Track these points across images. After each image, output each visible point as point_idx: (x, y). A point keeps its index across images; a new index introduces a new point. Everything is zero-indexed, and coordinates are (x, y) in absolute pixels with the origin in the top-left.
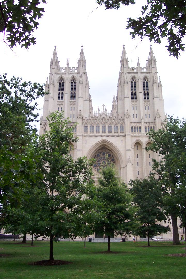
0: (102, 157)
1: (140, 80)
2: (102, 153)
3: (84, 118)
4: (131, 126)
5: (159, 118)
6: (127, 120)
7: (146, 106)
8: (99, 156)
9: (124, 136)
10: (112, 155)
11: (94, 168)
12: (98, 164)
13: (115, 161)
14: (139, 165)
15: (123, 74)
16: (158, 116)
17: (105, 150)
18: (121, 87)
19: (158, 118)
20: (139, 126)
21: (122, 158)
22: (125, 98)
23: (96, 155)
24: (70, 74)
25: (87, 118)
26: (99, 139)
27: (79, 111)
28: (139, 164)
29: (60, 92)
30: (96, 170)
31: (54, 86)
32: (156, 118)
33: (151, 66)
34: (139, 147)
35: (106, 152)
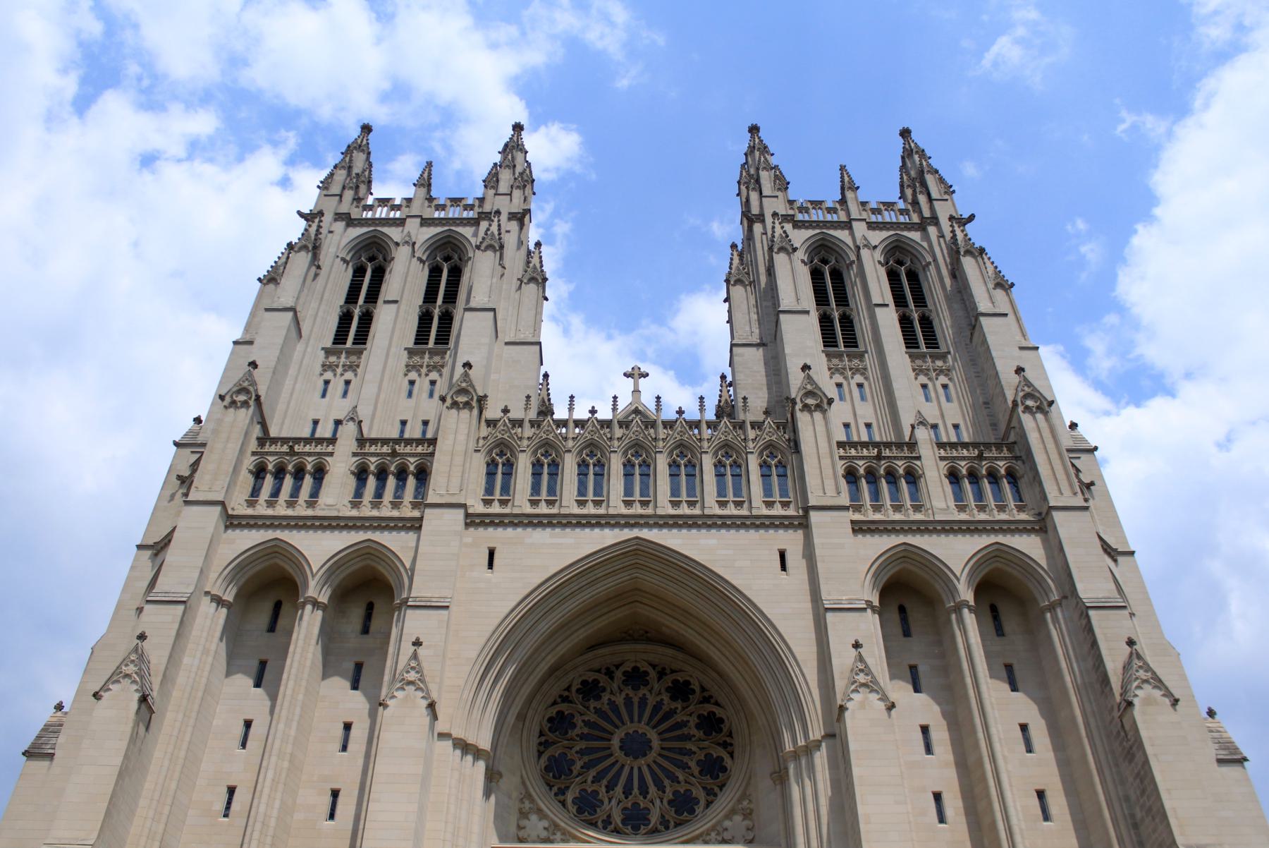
0: (620, 700)
1: (865, 253)
2: (619, 674)
3: (492, 412)
4: (841, 467)
5: (1039, 416)
7: (923, 379)
8: (598, 698)
10: (703, 689)
11: (551, 787)
12: (581, 753)
13: (730, 735)
16: (1030, 403)
17: (639, 647)
20: (901, 467)
23: (568, 689)
24: (426, 222)
25: (512, 415)
26: (609, 537)
27: (459, 370)
30: (570, 797)
33: (922, 199)
34: (916, 616)
35: (654, 666)
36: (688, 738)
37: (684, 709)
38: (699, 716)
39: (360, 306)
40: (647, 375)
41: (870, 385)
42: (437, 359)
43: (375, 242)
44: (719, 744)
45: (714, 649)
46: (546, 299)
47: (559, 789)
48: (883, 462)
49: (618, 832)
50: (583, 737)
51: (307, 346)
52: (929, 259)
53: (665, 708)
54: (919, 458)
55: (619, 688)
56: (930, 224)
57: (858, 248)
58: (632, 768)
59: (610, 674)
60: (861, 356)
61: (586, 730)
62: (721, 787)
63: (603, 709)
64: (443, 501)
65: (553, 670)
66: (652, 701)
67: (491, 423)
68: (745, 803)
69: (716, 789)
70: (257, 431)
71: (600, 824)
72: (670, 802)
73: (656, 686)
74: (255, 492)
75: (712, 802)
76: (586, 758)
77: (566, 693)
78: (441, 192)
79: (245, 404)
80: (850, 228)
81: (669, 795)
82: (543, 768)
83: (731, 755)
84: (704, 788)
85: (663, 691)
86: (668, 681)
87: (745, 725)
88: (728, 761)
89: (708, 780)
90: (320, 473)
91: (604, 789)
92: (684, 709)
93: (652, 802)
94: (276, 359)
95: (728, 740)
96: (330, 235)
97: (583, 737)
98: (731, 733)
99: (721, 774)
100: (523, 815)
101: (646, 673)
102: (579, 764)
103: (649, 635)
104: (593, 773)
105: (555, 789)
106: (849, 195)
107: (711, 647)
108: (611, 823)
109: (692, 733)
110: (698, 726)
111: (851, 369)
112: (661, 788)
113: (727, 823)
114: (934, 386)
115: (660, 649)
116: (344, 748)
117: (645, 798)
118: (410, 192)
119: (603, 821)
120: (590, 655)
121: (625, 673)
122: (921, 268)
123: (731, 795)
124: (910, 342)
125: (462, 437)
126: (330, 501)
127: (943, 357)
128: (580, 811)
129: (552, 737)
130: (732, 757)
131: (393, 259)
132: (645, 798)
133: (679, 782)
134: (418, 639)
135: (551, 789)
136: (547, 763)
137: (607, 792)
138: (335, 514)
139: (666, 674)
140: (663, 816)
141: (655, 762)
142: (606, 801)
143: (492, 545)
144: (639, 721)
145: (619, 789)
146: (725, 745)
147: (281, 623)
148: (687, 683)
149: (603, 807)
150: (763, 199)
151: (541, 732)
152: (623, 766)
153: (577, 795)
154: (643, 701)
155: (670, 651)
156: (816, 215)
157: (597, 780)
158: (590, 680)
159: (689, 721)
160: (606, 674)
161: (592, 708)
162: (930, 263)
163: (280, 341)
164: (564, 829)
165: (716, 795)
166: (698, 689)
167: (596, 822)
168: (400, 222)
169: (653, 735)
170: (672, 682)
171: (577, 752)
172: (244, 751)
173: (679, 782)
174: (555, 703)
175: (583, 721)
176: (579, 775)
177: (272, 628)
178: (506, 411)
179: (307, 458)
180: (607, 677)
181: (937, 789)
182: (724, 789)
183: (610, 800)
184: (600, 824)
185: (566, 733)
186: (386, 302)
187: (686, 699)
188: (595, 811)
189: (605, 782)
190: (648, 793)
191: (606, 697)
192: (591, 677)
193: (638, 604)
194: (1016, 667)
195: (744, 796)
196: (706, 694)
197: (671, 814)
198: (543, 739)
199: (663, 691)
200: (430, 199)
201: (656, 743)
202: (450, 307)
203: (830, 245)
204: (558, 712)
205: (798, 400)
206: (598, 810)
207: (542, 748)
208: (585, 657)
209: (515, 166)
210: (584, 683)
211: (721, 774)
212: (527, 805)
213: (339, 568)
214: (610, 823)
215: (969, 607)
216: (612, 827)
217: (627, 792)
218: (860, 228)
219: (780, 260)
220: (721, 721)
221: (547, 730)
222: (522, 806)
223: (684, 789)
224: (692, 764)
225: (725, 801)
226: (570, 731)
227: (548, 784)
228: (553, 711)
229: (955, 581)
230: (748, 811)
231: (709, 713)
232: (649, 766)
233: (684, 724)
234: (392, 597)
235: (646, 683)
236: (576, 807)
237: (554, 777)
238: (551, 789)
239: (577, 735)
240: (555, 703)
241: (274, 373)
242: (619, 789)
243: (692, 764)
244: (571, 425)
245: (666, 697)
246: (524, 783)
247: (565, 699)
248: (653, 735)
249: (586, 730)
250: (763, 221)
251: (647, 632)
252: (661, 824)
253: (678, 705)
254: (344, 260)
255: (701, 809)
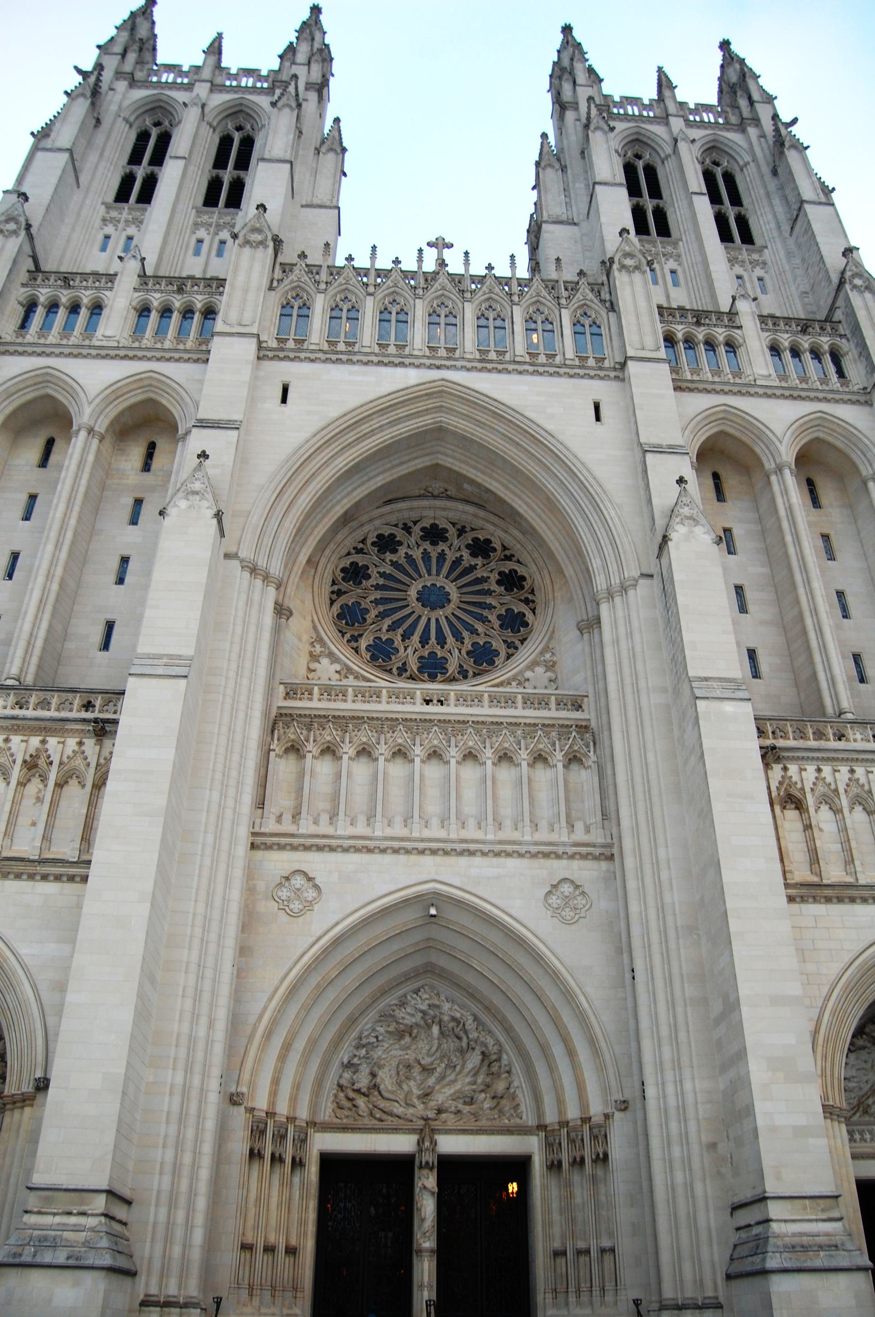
0: (417, 554)
1: (682, 146)
2: (417, 530)
3: (288, 255)
6: (632, 283)
7: (738, 270)
8: (394, 551)
9: (612, 374)
10: (505, 548)
11: (343, 634)
12: (376, 602)
13: (532, 592)
14: (751, 607)
15: (570, 115)
16: (858, 282)
17: (439, 503)
18: (564, 169)
19: (862, 292)
21: (610, 513)
22: (597, 187)
23: (363, 541)
24: (215, 87)
25: (309, 261)
28: (749, 595)
29: (134, 168)
30: (363, 644)
31: (98, 121)
32: (848, 286)
33: (743, 103)
36: (489, 592)
37: (484, 565)
38: (500, 574)
39: (144, 168)
40: (452, 246)
41: (684, 271)
42: (228, 219)
43: (161, 107)
44: (520, 600)
45: (520, 502)
46: (345, 175)
47: (351, 636)
48: (702, 328)
49: (413, 679)
50: (377, 587)
51: (85, 197)
52: (748, 158)
53: (465, 564)
54: (740, 327)
55: (417, 543)
56: (749, 125)
57: (676, 140)
58: (429, 619)
59: (407, 529)
60: (675, 244)
61: (381, 581)
62: (522, 641)
63: (400, 562)
64: (234, 330)
65: (346, 519)
66: (451, 556)
67: (287, 268)
68: (548, 656)
69: (517, 643)
70: (29, 264)
71: (394, 670)
72: (468, 653)
73: (456, 542)
74: (24, 325)
75: (512, 655)
76: (381, 608)
77: (361, 546)
78: (231, 60)
79: (15, 233)
80: (667, 124)
81: (468, 645)
82: (335, 615)
83: (534, 611)
84: (505, 641)
85: (462, 547)
86: (468, 538)
87: (548, 582)
88: (529, 617)
89: (508, 633)
90: (97, 308)
91: (400, 638)
92: (484, 565)
93: (450, 652)
94: (50, 197)
95: (530, 597)
96: (111, 93)
97: (377, 587)
98: (533, 590)
99: (522, 629)
100: (314, 657)
101: (445, 530)
102: (373, 613)
103: (449, 493)
104: (388, 622)
105: (348, 636)
106: (667, 93)
107: (516, 499)
108: (406, 671)
109: (492, 589)
110: (499, 582)
111: (664, 255)
112: (459, 638)
113: (528, 674)
114: (750, 277)
115: (460, 506)
116: (120, 581)
117: (442, 647)
118: (199, 59)
119: (398, 668)
120: (387, 508)
121: (423, 529)
122: (738, 169)
123: (534, 647)
124: (725, 236)
125: (255, 275)
126: (108, 333)
127: (761, 250)
128: (374, 658)
129: (344, 586)
130: (534, 613)
131: (180, 122)
132: (442, 647)
133: (478, 634)
134: (204, 452)
135: (343, 636)
136: (339, 611)
137: (402, 641)
138: (116, 344)
139: (466, 532)
140: (461, 666)
141: (453, 614)
142: (402, 649)
143: (286, 379)
144: (438, 575)
145: (416, 638)
146: (527, 601)
147: (53, 458)
148: (488, 542)
149: (400, 654)
150: (577, 88)
151: (333, 581)
152: (420, 617)
153: (371, 642)
154: (442, 556)
155: (470, 509)
156: (635, 110)
157: (392, 628)
158: (386, 534)
159: (489, 578)
160: (403, 529)
161: (387, 561)
162: (747, 164)
163: (54, 180)
164: (357, 673)
165: (516, 648)
166: (499, 548)
167: (391, 669)
168: (189, 87)
169: (452, 589)
170: (472, 540)
171: (371, 602)
172: (10, 582)
173: (478, 634)
174: (349, 554)
175: (378, 572)
176: (374, 623)
177: (44, 463)
178: (303, 256)
179: (83, 292)
180: (404, 532)
181: (752, 645)
182: (525, 643)
183: (406, 648)
184: (394, 670)
185: (361, 583)
186: (171, 157)
187: (486, 556)
188: (390, 659)
189: (400, 631)
190: (446, 643)
191: (402, 551)
192: (387, 531)
193: (440, 456)
194: (833, 538)
195: (546, 649)
196: (507, 553)
197: (469, 665)
198: (336, 588)
199: (462, 547)
200: (218, 66)
201: (454, 595)
202: (242, 173)
203: (645, 139)
204: (352, 564)
205: (616, 260)
206: (393, 657)
207: (334, 597)
208: (380, 510)
209: (313, 39)
210: (380, 537)
211: (522, 629)
212: (318, 649)
213: (117, 398)
214: (406, 671)
215: (790, 469)
216: (408, 674)
217: (424, 641)
218: (677, 124)
219: (597, 139)
220: (523, 578)
221: (340, 579)
222: (313, 650)
223: (484, 640)
224: (493, 618)
225: (526, 654)
226: (364, 582)
227: (340, 631)
228: (346, 562)
229: (777, 443)
230: (551, 663)
231: (510, 571)
232: (446, 617)
233: (485, 580)
234: (176, 429)
235: (445, 540)
236: (369, 654)
237: (347, 624)
238: (343, 636)
239: (372, 586)
240: (349, 554)
241: (47, 210)
242: (416, 638)
243: (493, 618)
244: (373, 274)
245: (466, 554)
246: (315, 628)
247: (359, 551)
248: (452, 589)
249: (381, 581)
250: (577, 109)
251: (446, 490)
252: (459, 673)
253: (479, 561)
254: (126, 120)
255: (502, 660)
